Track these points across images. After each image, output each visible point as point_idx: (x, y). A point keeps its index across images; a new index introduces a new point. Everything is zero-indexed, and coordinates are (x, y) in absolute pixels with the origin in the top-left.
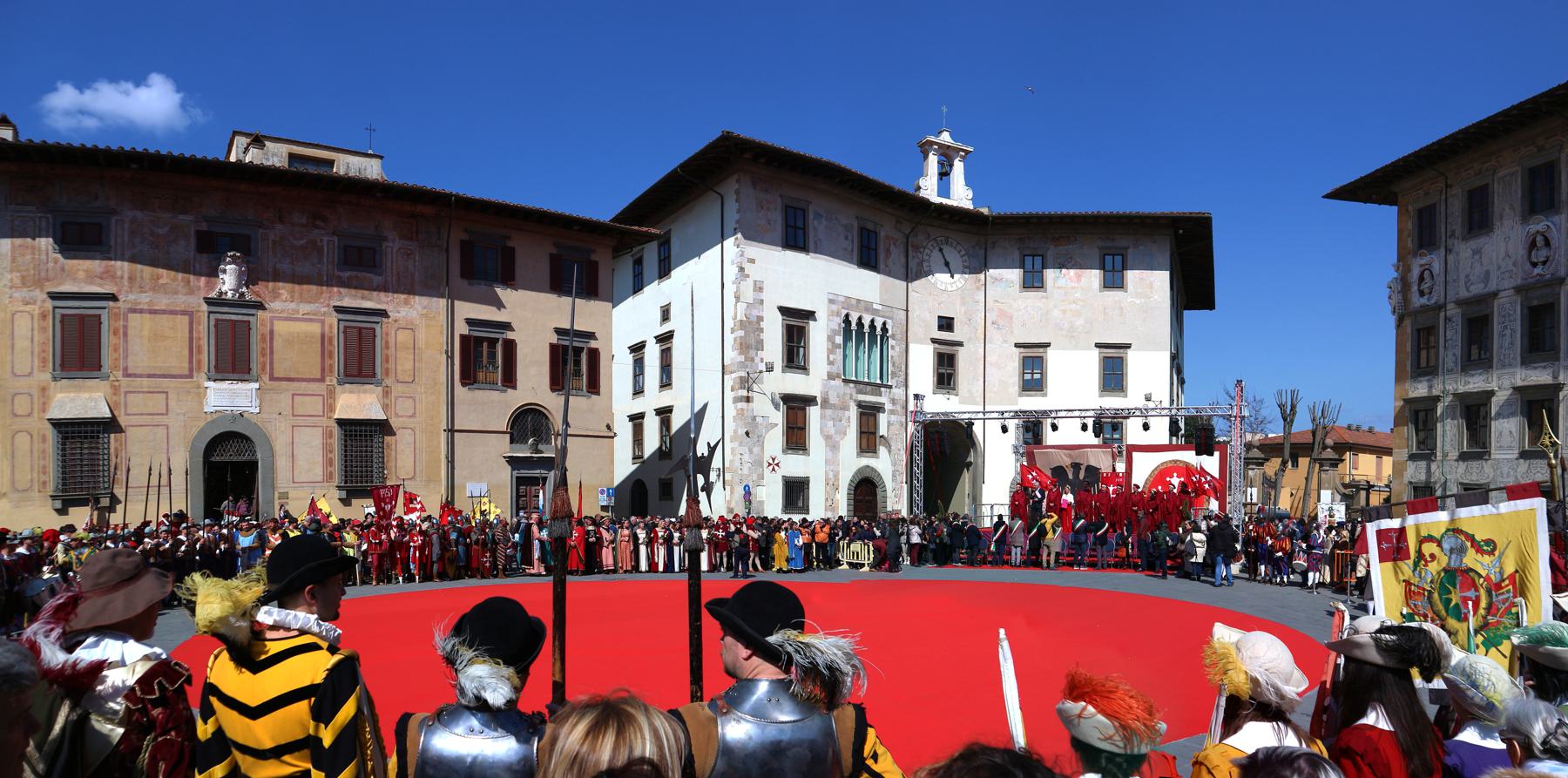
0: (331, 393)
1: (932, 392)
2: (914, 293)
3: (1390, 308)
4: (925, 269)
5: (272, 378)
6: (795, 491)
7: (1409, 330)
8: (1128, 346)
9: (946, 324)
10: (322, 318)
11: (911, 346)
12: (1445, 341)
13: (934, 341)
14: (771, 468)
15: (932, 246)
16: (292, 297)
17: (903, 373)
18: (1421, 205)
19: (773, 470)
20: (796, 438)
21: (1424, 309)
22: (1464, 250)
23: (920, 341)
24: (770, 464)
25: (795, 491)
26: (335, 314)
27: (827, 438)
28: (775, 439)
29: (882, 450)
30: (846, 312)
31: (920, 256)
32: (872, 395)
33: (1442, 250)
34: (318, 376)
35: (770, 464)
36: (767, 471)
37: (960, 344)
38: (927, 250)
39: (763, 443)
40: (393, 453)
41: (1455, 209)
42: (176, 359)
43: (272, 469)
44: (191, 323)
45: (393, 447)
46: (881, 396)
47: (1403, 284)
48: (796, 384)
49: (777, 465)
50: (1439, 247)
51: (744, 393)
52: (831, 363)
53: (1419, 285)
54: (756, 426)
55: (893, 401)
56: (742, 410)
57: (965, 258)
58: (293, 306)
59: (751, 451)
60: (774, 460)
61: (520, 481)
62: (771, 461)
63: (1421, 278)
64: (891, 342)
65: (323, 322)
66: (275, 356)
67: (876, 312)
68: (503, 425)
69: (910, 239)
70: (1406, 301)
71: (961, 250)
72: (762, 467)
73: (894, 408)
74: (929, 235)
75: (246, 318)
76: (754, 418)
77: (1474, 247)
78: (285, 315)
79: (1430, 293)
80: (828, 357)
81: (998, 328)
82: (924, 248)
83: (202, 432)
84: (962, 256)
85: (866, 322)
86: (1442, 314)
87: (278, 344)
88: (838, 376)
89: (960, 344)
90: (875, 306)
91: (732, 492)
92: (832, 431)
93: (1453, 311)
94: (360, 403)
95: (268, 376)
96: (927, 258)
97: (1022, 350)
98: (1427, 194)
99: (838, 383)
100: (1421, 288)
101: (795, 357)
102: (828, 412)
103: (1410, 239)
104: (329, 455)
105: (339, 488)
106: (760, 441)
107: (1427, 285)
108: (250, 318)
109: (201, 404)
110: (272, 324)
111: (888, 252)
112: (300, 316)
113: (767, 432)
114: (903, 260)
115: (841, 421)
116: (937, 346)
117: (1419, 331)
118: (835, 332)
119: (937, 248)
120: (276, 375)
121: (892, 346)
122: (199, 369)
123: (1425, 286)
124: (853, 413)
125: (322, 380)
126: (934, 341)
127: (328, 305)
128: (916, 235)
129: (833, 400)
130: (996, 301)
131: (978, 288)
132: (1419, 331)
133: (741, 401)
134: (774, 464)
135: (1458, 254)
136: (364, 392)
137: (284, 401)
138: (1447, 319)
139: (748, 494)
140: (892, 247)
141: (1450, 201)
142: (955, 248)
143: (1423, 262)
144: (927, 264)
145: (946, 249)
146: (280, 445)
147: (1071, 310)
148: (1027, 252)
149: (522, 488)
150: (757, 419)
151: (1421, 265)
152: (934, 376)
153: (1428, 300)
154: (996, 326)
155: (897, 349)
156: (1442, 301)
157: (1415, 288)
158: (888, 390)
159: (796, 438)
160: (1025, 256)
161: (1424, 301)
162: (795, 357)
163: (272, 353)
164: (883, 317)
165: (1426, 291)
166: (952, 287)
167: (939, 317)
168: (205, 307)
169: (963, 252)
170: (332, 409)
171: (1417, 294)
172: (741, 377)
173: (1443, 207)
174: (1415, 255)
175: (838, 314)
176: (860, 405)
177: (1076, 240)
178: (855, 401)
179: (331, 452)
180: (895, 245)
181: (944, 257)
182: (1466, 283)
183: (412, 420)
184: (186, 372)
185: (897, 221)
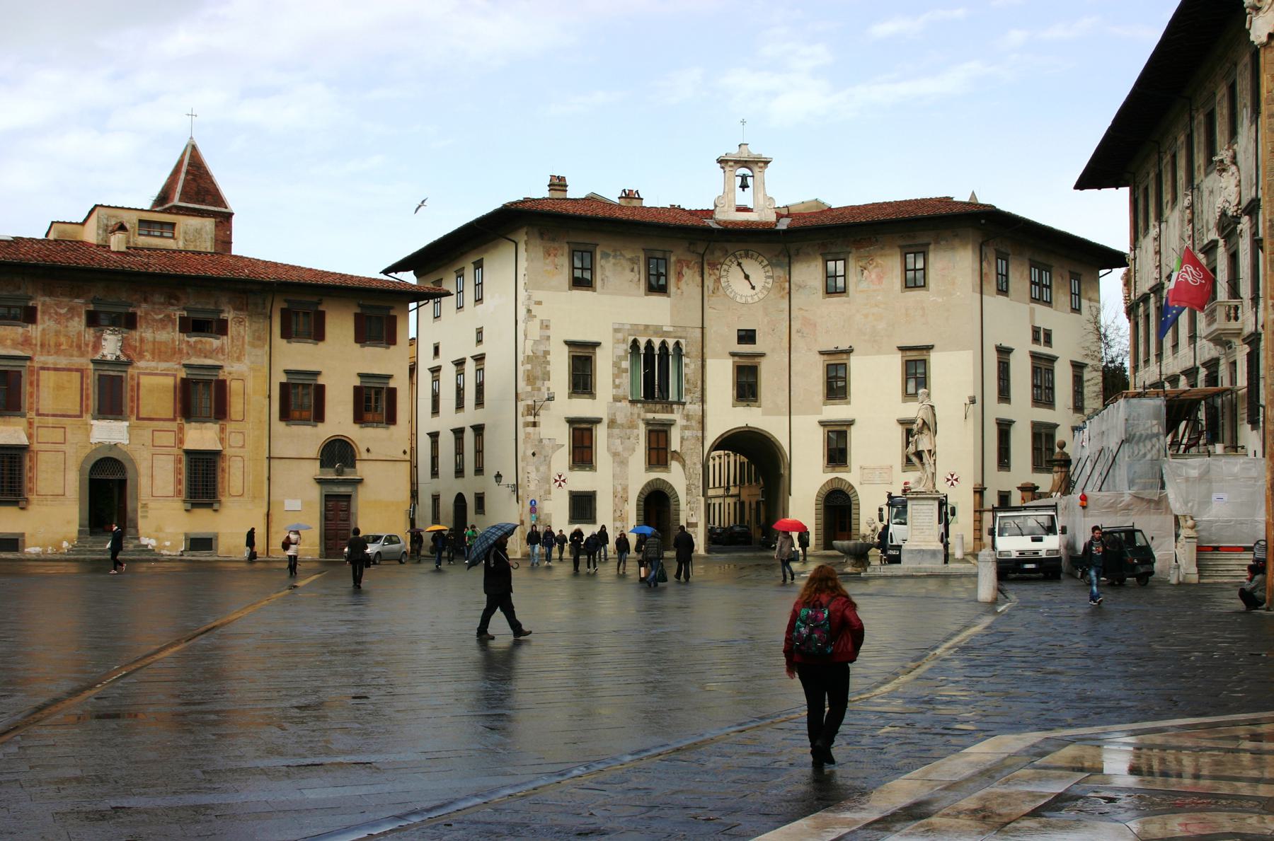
0: (181, 429)
2: (710, 310)
4: (723, 285)
5: (138, 418)
6: (582, 505)
8: (929, 348)
9: (747, 336)
11: (710, 363)
13: (733, 355)
14: (558, 484)
15: (730, 261)
16: (153, 358)
17: (699, 389)
19: (560, 485)
20: (582, 454)
23: (717, 356)
24: (556, 481)
25: (582, 505)
26: (184, 369)
27: (615, 455)
28: (561, 459)
29: (675, 465)
30: (633, 338)
31: (717, 272)
32: (663, 412)
34: (172, 417)
35: (556, 481)
36: (554, 487)
37: (762, 355)
38: (725, 267)
39: (550, 462)
40: (227, 476)
42: (71, 402)
43: (136, 486)
44: (82, 378)
45: (227, 471)
46: (672, 412)
48: (582, 408)
51: (531, 419)
52: (616, 386)
54: (543, 447)
55: (688, 417)
56: (529, 434)
57: (768, 268)
58: (153, 364)
59: (538, 470)
60: (560, 476)
61: (328, 498)
62: (557, 478)
64: (685, 360)
65: (175, 376)
66: (140, 402)
67: (668, 334)
68: (314, 450)
69: (705, 258)
71: (762, 261)
72: (549, 484)
73: (689, 423)
74: (727, 251)
75: (120, 374)
76: (541, 441)
78: (148, 371)
80: (614, 381)
81: (803, 337)
82: (722, 264)
83: (88, 457)
84: (764, 267)
85: (657, 343)
87: (143, 392)
88: (625, 398)
89: (762, 355)
90: (665, 329)
91: (523, 507)
92: (620, 449)
94: (202, 437)
95: (135, 417)
96: (725, 273)
97: (825, 357)
99: (625, 404)
101: (582, 381)
102: (616, 431)
104: (179, 477)
105: (185, 501)
106: (547, 461)
108: (124, 374)
109: (88, 436)
110: (138, 378)
111: (680, 275)
112: (159, 372)
113: (553, 452)
114: (700, 279)
115: (629, 438)
116: (736, 359)
118: (620, 358)
119: (736, 263)
120: (141, 416)
121: (685, 364)
122: (87, 411)
124: (642, 430)
125: (174, 419)
126: (733, 355)
127: (179, 363)
128: (712, 253)
129: (620, 419)
130: (801, 309)
131: (783, 297)
133: (528, 426)
134: (560, 481)
136: (206, 428)
137: (147, 434)
139: (533, 509)
140: (685, 270)
144: (725, 280)
145: (745, 262)
146: (143, 468)
147: (873, 314)
149: (330, 504)
150: (544, 441)
152: (733, 389)
154: (800, 334)
155: (692, 366)
158: (681, 407)
159: (582, 454)
162: (582, 381)
163: (138, 399)
164: (675, 337)
166: (753, 299)
167: (738, 330)
168: (91, 366)
169: (766, 262)
170: (181, 441)
172: (528, 405)
175: (624, 341)
176: (647, 423)
177: (877, 241)
178: (643, 420)
179: (180, 474)
180: (688, 267)
181: (743, 270)
183: (242, 449)
184: (78, 413)
185: (690, 244)
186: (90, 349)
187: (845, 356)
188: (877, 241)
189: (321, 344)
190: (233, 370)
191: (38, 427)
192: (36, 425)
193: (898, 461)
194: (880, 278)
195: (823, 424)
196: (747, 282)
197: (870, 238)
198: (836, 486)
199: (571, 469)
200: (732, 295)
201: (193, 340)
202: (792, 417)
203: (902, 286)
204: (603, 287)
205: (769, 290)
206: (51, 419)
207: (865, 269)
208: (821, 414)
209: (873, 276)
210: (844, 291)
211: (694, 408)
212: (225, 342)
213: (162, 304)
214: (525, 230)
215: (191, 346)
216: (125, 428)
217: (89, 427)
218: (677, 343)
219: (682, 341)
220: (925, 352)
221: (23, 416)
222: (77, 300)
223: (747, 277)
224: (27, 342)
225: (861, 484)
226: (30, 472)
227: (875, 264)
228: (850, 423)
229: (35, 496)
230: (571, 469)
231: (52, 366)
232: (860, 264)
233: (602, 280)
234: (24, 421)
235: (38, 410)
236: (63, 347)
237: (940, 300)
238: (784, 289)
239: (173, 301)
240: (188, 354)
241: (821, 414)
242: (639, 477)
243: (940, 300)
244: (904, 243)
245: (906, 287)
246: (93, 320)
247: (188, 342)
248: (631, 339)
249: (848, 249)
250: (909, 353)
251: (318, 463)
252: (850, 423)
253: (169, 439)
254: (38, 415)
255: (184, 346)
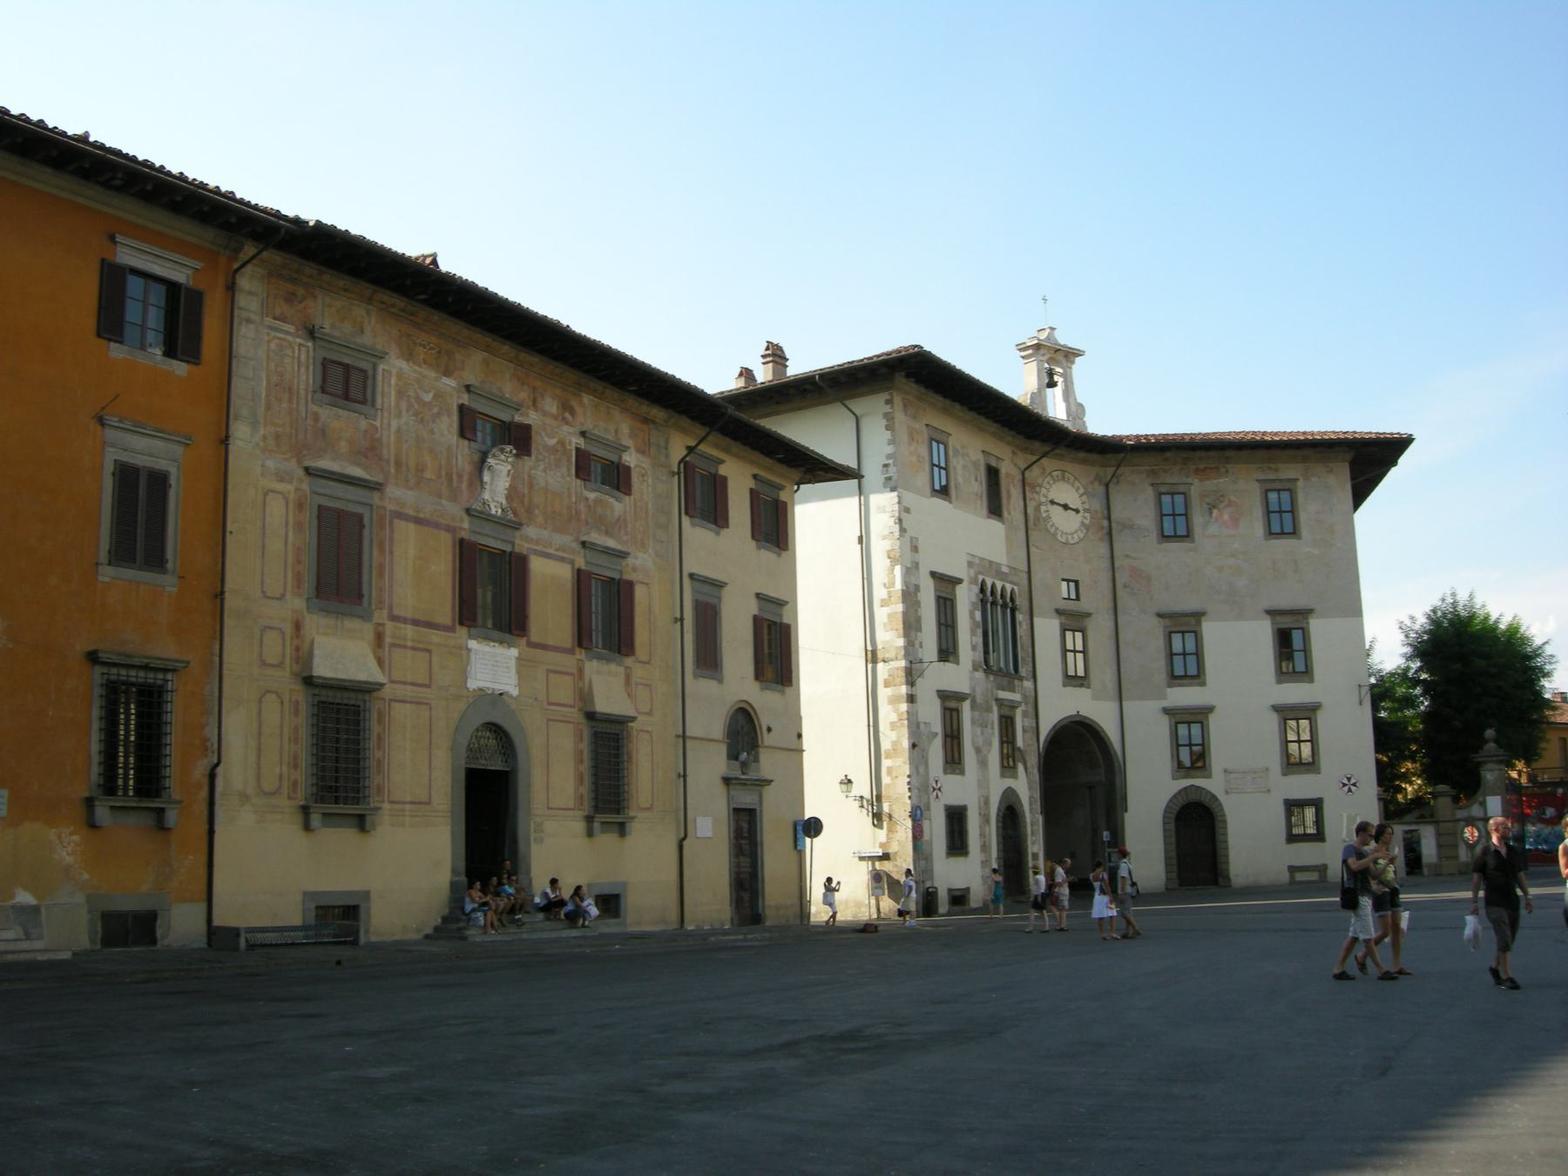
1: (1061, 683)
10: (572, 557)
15: (1049, 483)
27: (978, 750)
31: (1036, 497)
35: (934, 789)
37: (1089, 615)
38: (1044, 490)
46: (1014, 692)
49: (939, 789)
57: (1084, 498)
58: (545, 534)
74: (1044, 469)
80: (971, 639)
82: (1040, 486)
85: (999, 585)
97: (1167, 622)
125: (571, 652)
142: (1073, 485)
148: (1163, 489)
160: (1161, 494)
169: (1082, 491)
186: (464, 486)
187: (1193, 621)
188: (1227, 471)
189: (724, 532)
190: (638, 562)
191: (393, 645)
192: (388, 640)
193: (1275, 763)
194: (1235, 521)
195: (1167, 711)
196: (1069, 511)
197: (1217, 468)
198: (1193, 797)
199: (945, 772)
200: (1052, 530)
201: (592, 496)
202: (1124, 703)
203: (1265, 531)
204: (957, 497)
205: (1087, 528)
206: (409, 631)
207: (1214, 507)
208: (1165, 698)
209: (1226, 517)
210: (1188, 536)
211: (1028, 684)
212: (628, 509)
213: (555, 418)
214: (885, 396)
215: (590, 506)
216: (513, 663)
217: (464, 652)
218: (1012, 590)
219: (1016, 588)
220: (1300, 618)
221: (366, 617)
222: (446, 380)
223: (1066, 507)
224: (370, 450)
225: (1227, 792)
226: (379, 748)
227: (1226, 502)
228: (1209, 710)
229: (386, 806)
230: (945, 772)
231: (411, 513)
232: (1207, 500)
233: (956, 487)
234: (368, 630)
235: (391, 608)
236: (428, 475)
237: (1316, 552)
238: (1102, 528)
239: (567, 415)
240: (587, 523)
241: (1165, 698)
242: (998, 786)
243: (1316, 552)
244: (1262, 477)
245: (1271, 534)
246: (467, 422)
247: (587, 499)
248: (981, 578)
249: (1189, 480)
250: (1279, 619)
251: (723, 749)
252: (1209, 710)
253: (564, 691)
254: (394, 618)
255: (582, 507)
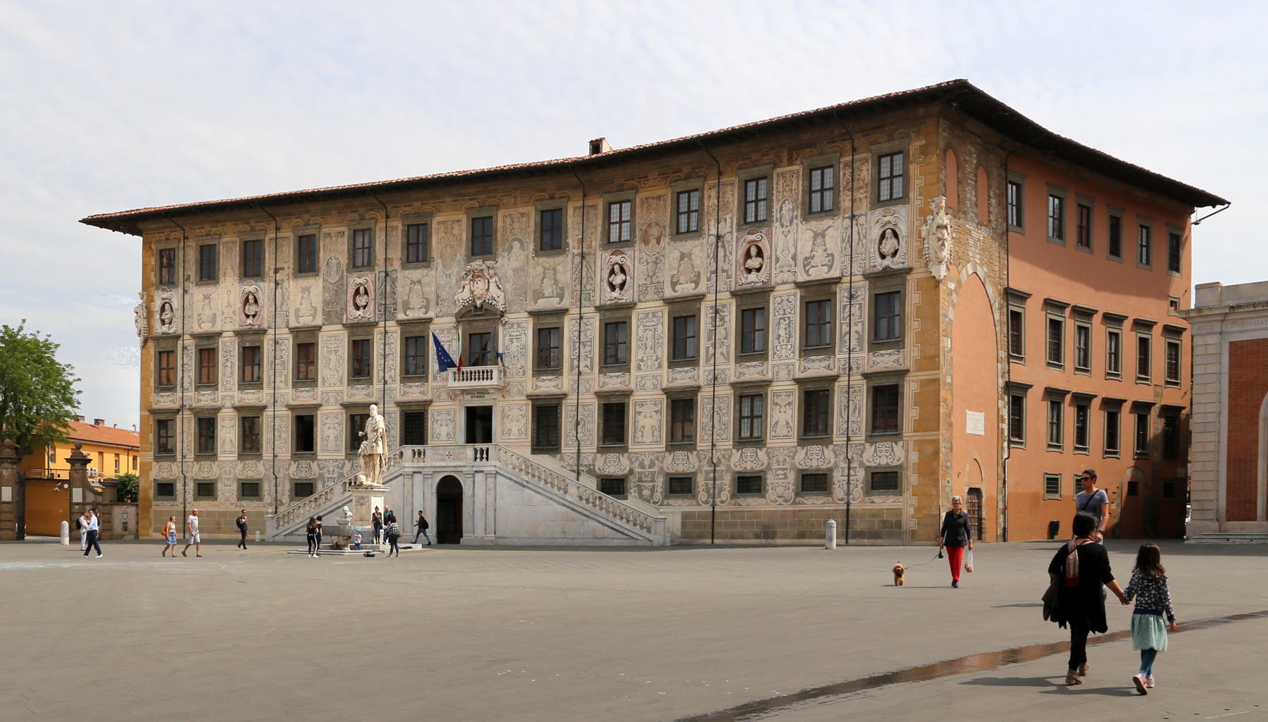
3: (136, 331)
7: (153, 353)
12: (183, 365)
18: (162, 246)
21: (166, 337)
22: (197, 293)
33: (180, 290)
41: (189, 259)
47: (147, 313)
50: (177, 286)
53: (161, 315)
63: (163, 309)
70: (150, 326)
77: (205, 293)
79: (170, 323)
86: (180, 343)
93: (190, 342)
98: (167, 239)
100: (163, 318)
103: (153, 274)
107: (168, 316)
117: (160, 353)
123: (166, 316)
132: (160, 353)
135: (192, 295)
138: (184, 348)
141: (187, 249)
143: (165, 296)
151: (163, 299)
153: (169, 329)
156: (180, 332)
157: (157, 316)
161: (165, 329)
165: (167, 321)
171: (159, 321)
173: (181, 253)
174: (157, 289)
182: (199, 320)
